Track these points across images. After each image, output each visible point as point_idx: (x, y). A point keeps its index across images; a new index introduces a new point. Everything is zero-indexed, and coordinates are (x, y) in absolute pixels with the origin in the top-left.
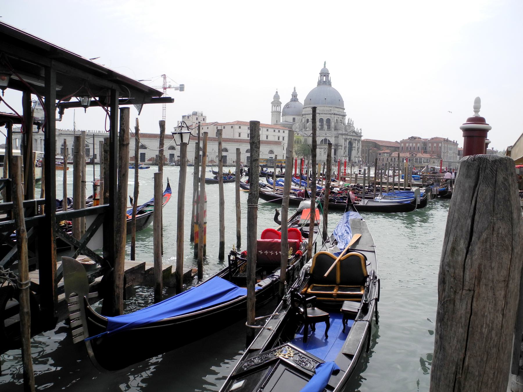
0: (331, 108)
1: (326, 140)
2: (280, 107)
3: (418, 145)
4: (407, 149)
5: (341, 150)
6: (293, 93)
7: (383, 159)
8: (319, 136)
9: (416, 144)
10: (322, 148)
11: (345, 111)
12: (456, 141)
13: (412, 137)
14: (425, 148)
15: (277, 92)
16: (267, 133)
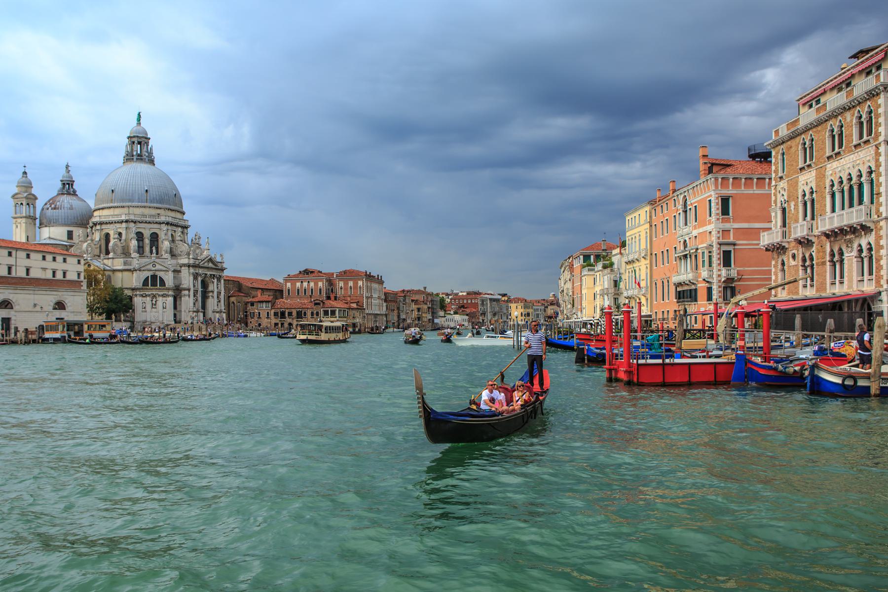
0: (158, 211)
1: (154, 277)
2: (34, 207)
3: (320, 284)
4: (298, 294)
5: (187, 297)
6: (63, 177)
7: (259, 313)
8: (140, 270)
9: (316, 284)
10: (146, 296)
11: (185, 217)
12: (381, 277)
13: (306, 270)
14: (332, 290)
15: (25, 173)
16: (27, 263)
